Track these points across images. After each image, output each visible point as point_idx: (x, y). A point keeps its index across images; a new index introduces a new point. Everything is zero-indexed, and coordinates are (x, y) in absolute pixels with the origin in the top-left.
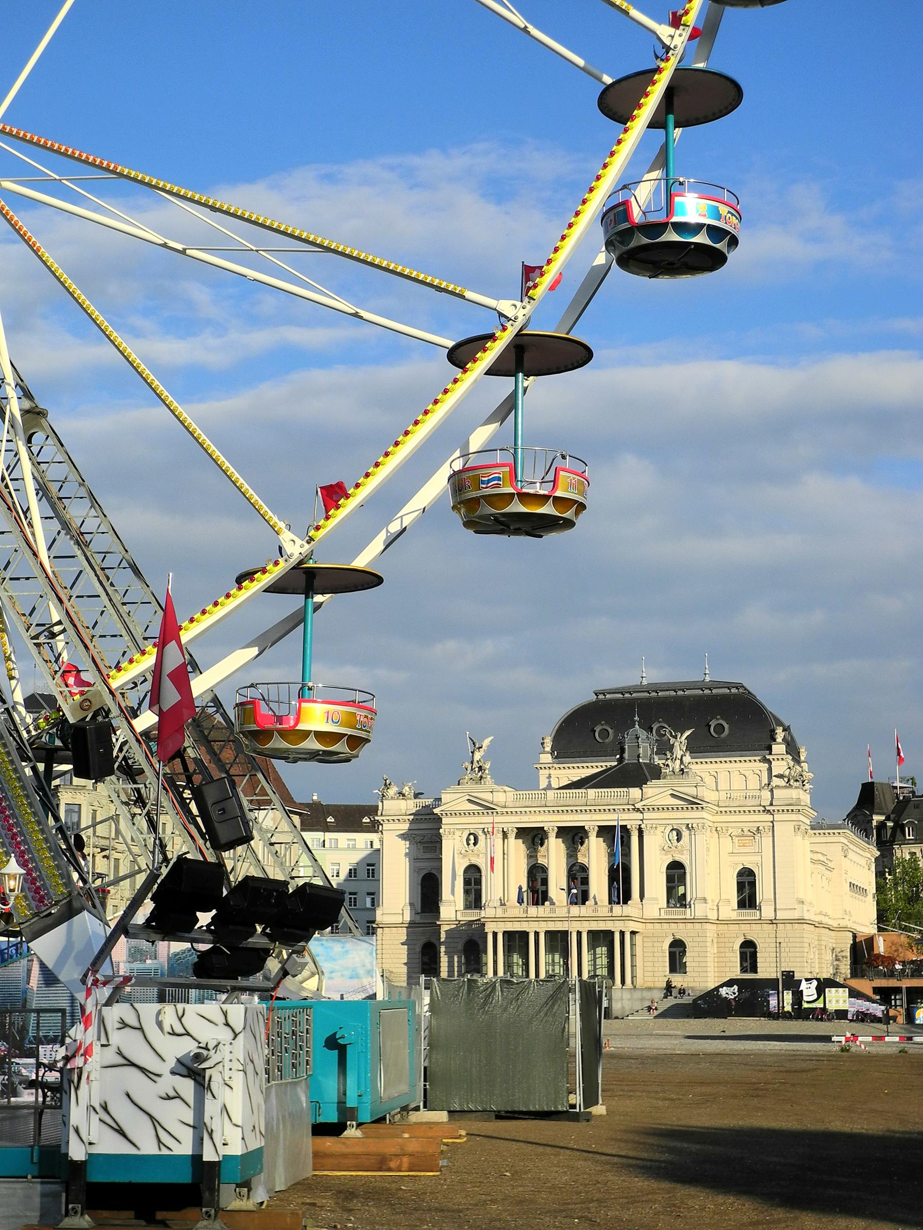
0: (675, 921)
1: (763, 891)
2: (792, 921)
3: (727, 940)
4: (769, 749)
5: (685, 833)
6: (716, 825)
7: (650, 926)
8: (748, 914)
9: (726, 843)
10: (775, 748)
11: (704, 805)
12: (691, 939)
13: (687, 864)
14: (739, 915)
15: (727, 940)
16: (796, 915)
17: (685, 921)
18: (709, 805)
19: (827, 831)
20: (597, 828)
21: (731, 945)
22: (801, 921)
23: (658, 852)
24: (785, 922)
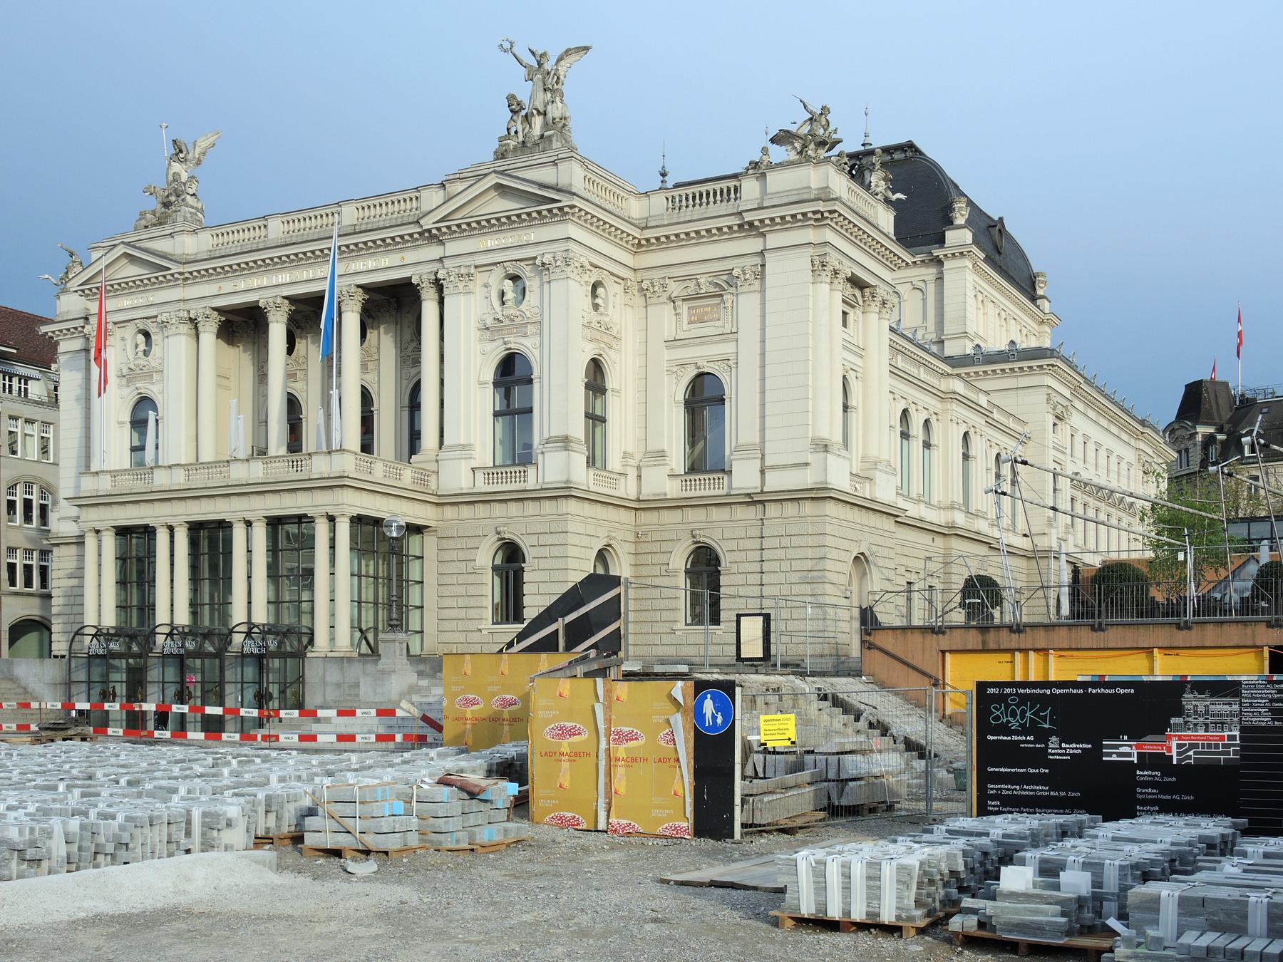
0: (504, 499)
1: (739, 421)
3: (655, 547)
4: (941, 241)
5: (532, 284)
6: (639, 276)
7: (450, 512)
8: (705, 487)
9: (666, 320)
10: (951, 236)
11: (566, 201)
13: (534, 356)
14: (685, 486)
15: (655, 547)
16: (806, 479)
17: (521, 498)
18: (576, 202)
19: (1017, 365)
20: (360, 296)
22: (821, 495)
23: (475, 334)
24: (783, 498)
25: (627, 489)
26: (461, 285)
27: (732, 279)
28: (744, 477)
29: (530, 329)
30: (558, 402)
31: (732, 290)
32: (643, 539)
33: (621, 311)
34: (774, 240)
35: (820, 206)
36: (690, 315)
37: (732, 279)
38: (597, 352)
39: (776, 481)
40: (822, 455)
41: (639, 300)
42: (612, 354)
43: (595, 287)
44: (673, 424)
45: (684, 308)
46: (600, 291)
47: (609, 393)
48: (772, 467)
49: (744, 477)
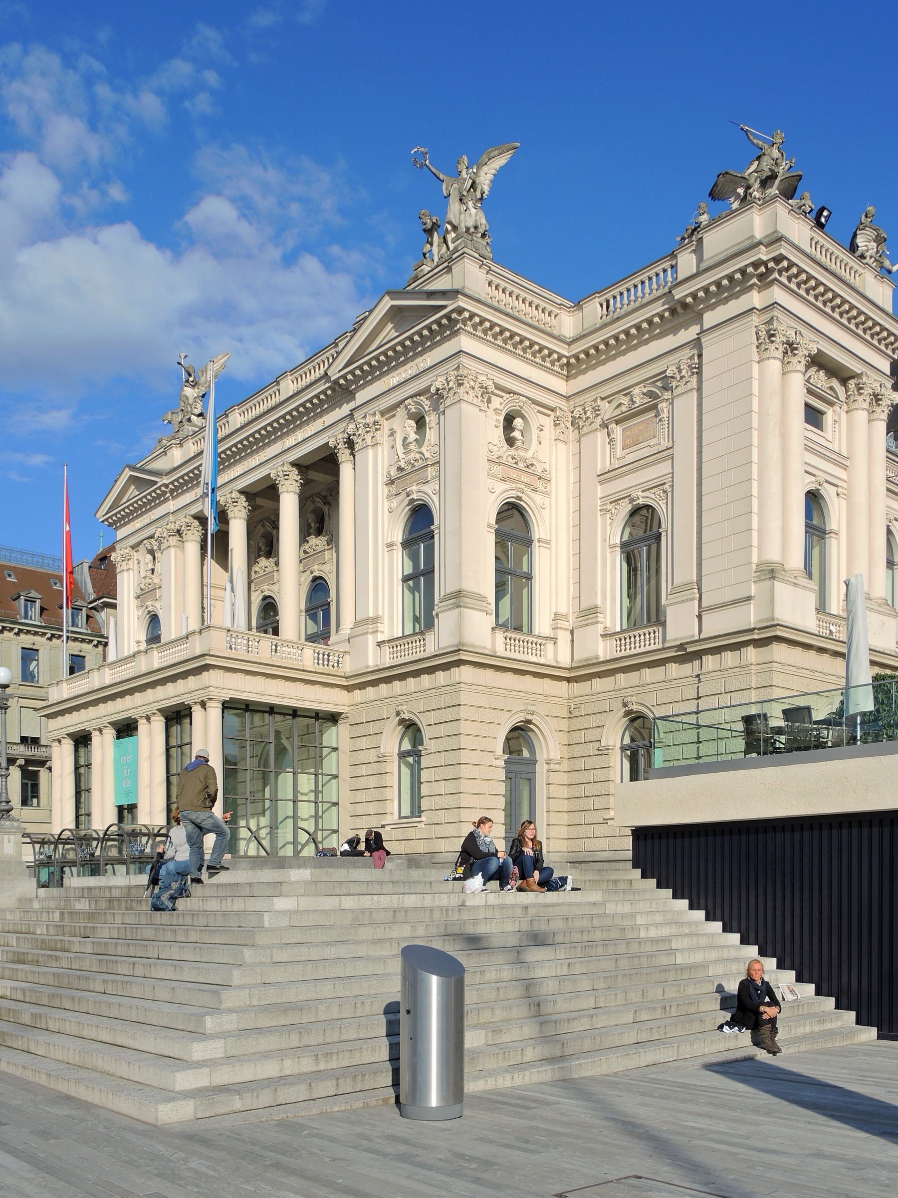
2: (736, 643)
8: (647, 642)
9: (602, 451)
12: (432, 718)
16: (750, 617)
21: (592, 735)
25: (560, 655)
26: (368, 438)
27: (665, 382)
28: (681, 625)
29: (431, 472)
30: (469, 556)
31: (667, 395)
32: (576, 713)
33: (549, 448)
34: (710, 318)
35: (763, 254)
36: (624, 440)
37: (665, 382)
38: (514, 493)
39: (718, 624)
40: (767, 583)
41: (572, 434)
42: (538, 498)
43: (509, 420)
44: (610, 572)
45: (618, 431)
46: (518, 422)
47: (536, 544)
48: (710, 609)
49: (681, 625)
